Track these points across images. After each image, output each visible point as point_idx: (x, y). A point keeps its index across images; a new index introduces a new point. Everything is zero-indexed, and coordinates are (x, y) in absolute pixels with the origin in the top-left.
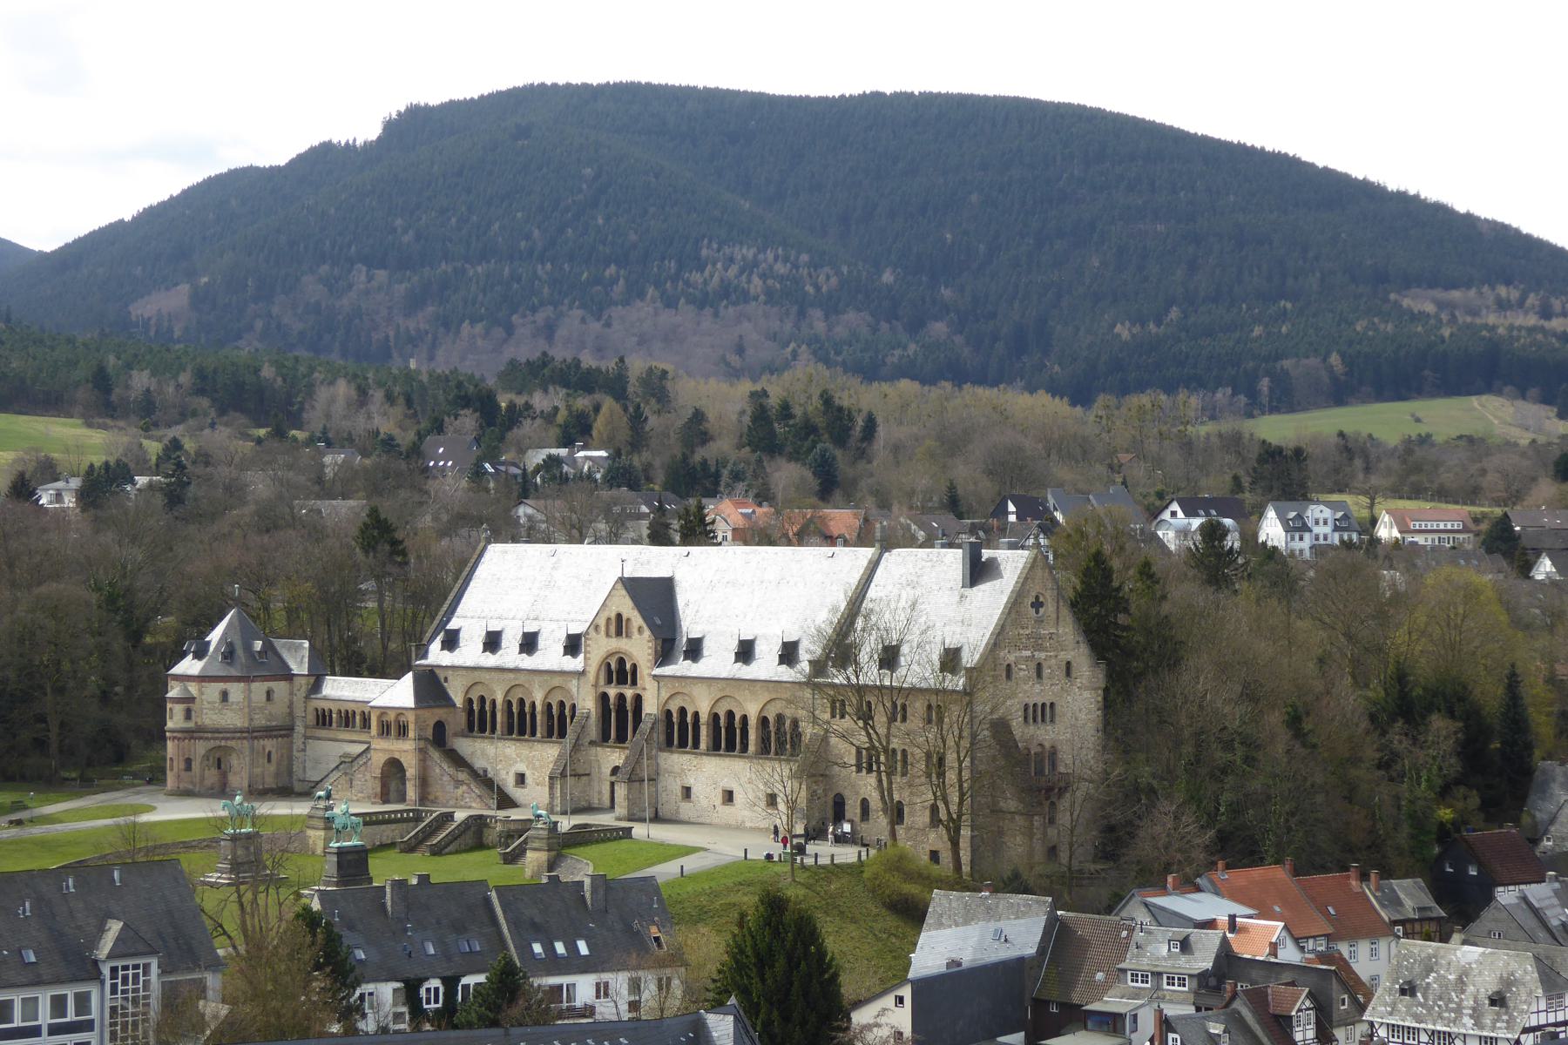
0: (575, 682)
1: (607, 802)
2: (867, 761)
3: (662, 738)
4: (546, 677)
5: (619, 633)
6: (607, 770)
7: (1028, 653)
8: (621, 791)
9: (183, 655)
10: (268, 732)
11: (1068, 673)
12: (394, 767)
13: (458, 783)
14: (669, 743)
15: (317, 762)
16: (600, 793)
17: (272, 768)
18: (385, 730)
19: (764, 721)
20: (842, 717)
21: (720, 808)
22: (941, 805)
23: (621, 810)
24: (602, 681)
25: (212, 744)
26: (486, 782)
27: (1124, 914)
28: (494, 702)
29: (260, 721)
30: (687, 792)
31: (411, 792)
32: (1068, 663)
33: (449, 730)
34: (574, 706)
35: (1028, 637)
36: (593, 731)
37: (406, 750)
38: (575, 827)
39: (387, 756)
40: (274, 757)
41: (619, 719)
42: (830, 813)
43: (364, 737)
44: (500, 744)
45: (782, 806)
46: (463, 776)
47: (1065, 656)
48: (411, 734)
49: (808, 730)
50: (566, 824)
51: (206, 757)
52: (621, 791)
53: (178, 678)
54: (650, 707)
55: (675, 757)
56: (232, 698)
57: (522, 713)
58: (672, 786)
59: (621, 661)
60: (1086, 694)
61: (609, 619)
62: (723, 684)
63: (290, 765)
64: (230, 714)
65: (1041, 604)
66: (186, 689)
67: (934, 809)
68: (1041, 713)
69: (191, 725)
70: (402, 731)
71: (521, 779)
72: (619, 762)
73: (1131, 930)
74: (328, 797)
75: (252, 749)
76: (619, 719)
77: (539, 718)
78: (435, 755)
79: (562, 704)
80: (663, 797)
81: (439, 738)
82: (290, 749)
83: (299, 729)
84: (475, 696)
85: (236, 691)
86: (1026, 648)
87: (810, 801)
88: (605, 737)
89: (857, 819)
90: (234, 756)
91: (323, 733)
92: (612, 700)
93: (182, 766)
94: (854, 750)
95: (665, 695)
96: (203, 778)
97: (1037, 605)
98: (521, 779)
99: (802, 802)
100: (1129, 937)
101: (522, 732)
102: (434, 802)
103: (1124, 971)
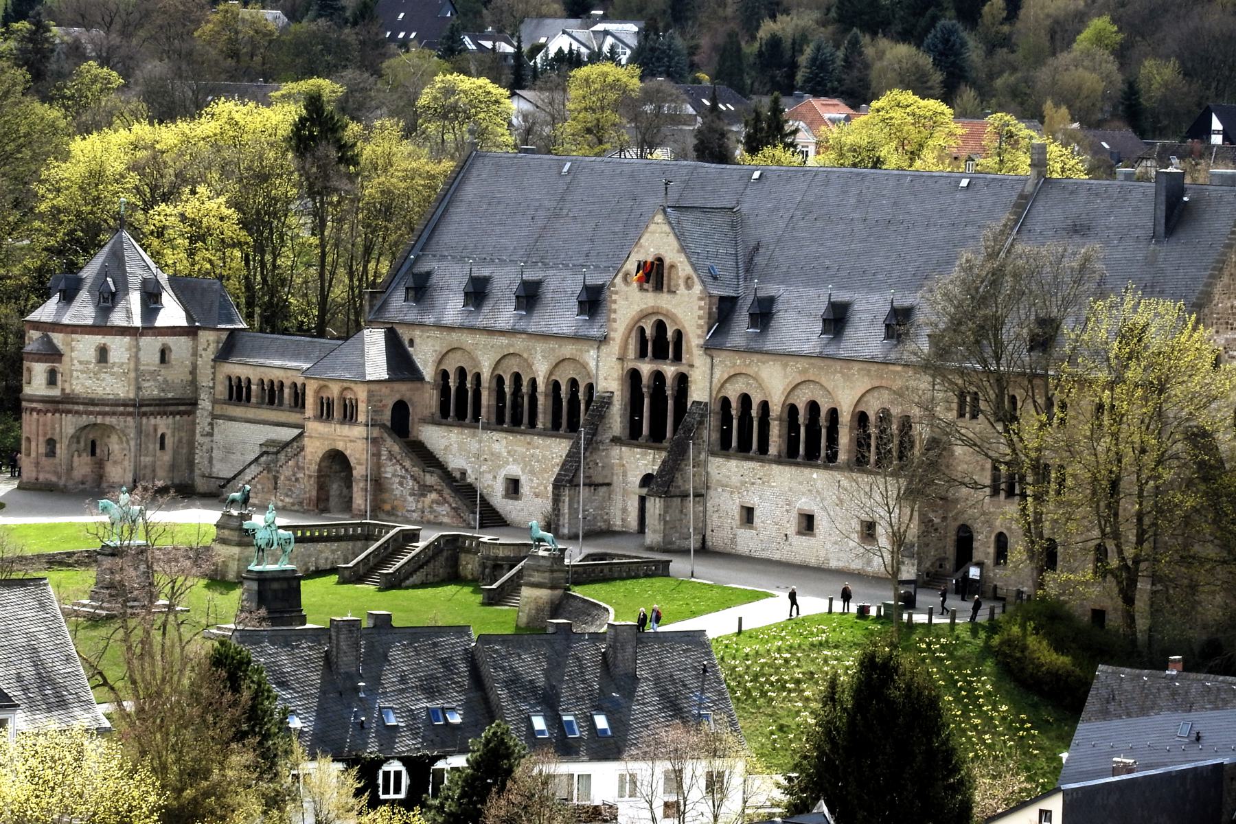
0: (593, 353)
1: (633, 522)
2: (1007, 484)
3: (715, 436)
4: (552, 344)
5: (659, 287)
6: (635, 479)
9: (45, 295)
10: (162, 406)
12: (337, 461)
13: (424, 489)
14: (725, 444)
15: (229, 450)
16: (624, 510)
17: (166, 457)
18: (325, 411)
20: (974, 416)
21: (796, 540)
22: (1111, 546)
24: (632, 352)
26: (463, 490)
28: (478, 377)
29: (151, 390)
30: (748, 514)
31: (360, 500)
33: (415, 413)
34: (590, 387)
36: (616, 420)
37: (352, 439)
41: (658, 411)
42: (951, 552)
43: (294, 417)
44: (486, 436)
45: (884, 541)
46: (431, 479)
48: (362, 418)
49: (922, 432)
50: (575, 555)
51: (76, 438)
53: (37, 325)
54: (698, 393)
55: (733, 464)
56: (113, 357)
59: (660, 327)
62: (802, 364)
63: (191, 453)
64: (109, 379)
66: (50, 342)
69: (55, 392)
70: (349, 415)
71: (513, 487)
72: (654, 469)
74: (245, 500)
75: (139, 431)
77: (541, 400)
78: (391, 445)
80: (714, 520)
81: (399, 421)
82: (193, 433)
83: (205, 404)
84: (451, 366)
85: (119, 347)
87: (923, 534)
89: (989, 562)
90: (114, 438)
91: (238, 411)
93: (42, 449)
94: (989, 465)
95: (719, 375)
96: (70, 468)
98: (513, 487)
101: (516, 421)
102: (392, 513)
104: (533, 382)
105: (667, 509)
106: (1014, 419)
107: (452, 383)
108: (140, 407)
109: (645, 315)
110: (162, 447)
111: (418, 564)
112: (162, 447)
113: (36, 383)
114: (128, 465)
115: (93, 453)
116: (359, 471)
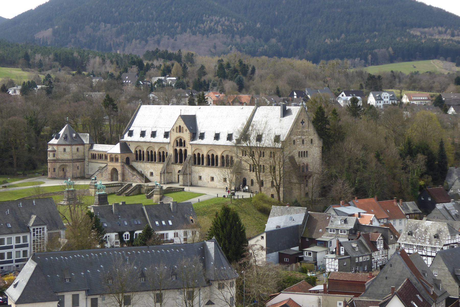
0: (167, 146)
1: (177, 181)
2: (253, 168)
3: (193, 162)
4: (159, 144)
5: (180, 131)
7: (300, 137)
8: (181, 177)
9: (52, 138)
10: (78, 160)
11: (312, 143)
12: (115, 171)
13: (133, 175)
14: (195, 163)
16: (175, 178)
17: (79, 171)
18: (112, 160)
19: (223, 157)
20: (245, 156)
22: (274, 181)
23: (181, 183)
25: (61, 164)
26: (142, 175)
27: (328, 212)
28: (143, 151)
29: (75, 157)
30: (200, 178)
31: (120, 178)
32: (312, 140)
34: (167, 153)
35: (300, 132)
36: (173, 160)
37: (118, 166)
38: (168, 188)
39: (112, 167)
40: (79, 168)
41: (180, 157)
44: (146, 164)
45: (228, 182)
46: (135, 173)
47: (310, 137)
48: (119, 161)
49: (235, 159)
50: (165, 187)
51: (60, 168)
52: (181, 177)
53: (51, 145)
54: (189, 153)
56: (67, 150)
57: (152, 155)
58: (195, 176)
59: (181, 140)
60: (317, 148)
61: (177, 127)
62: (210, 146)
65: (304, 122)
67: (272, 182)
68: (304, 154)
69: (55, 158)
70: (117, 160)
73: (330, 217)
74: (95, 179)
75: (73, 165)
76: (180, 157)
77: (157, 156)
78: (127, 167)
79: (163, 152)
80: (193, 179)
81: (128, 161)
84: (138, 150)
85: (68, 148)
86: (299, 135)
88: (176, 162)
89: (250, 185)
92: (178, 151)
93: (53, 170)
94: (249, 165)
95: (193, 149)
96: (59, 174)
97: (302, 122)
98: (152, 174)
99: (234, 180)
100: (329, 219)
101: (152, 160)
102: (126, 181)
103: (328, 229)
104: (155, 152)
105: (183, 177)
106: (254, 156)
107: (138, 153)
108: (73, 161)
109: (178, 138)
110: (78, 169)
111: (132, 191)
112: (78, 169)
113: (50, 157)
114: (71, 173)
115: (63, 171)
116: (119, 172)
